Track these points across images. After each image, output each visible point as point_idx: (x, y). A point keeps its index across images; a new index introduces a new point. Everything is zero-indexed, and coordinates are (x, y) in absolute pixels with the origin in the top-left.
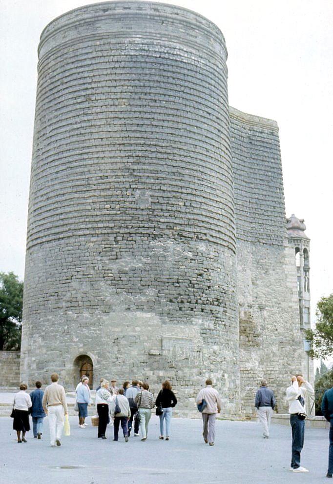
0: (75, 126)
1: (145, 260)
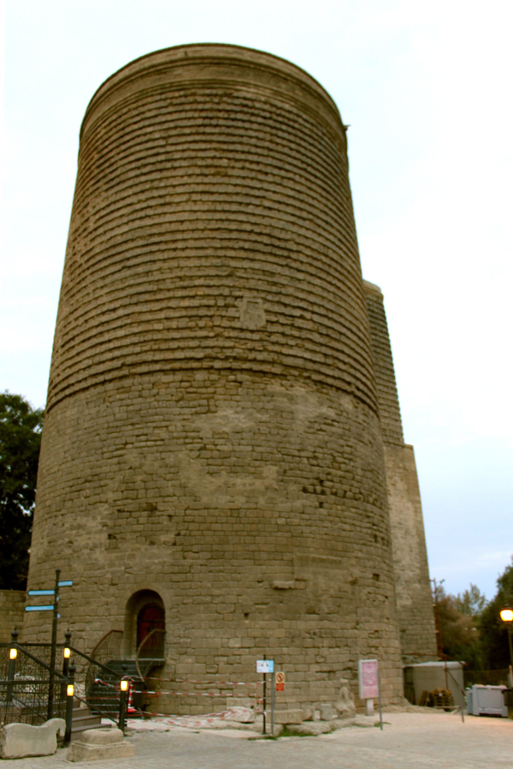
0: (138, 207)
1: (259, 416)
